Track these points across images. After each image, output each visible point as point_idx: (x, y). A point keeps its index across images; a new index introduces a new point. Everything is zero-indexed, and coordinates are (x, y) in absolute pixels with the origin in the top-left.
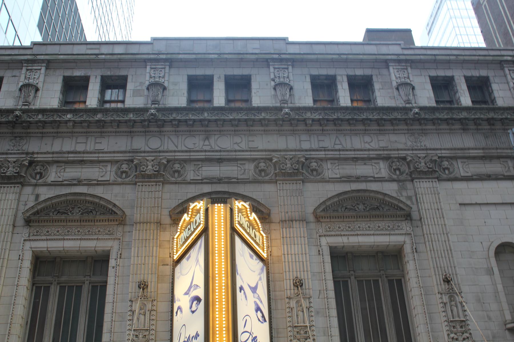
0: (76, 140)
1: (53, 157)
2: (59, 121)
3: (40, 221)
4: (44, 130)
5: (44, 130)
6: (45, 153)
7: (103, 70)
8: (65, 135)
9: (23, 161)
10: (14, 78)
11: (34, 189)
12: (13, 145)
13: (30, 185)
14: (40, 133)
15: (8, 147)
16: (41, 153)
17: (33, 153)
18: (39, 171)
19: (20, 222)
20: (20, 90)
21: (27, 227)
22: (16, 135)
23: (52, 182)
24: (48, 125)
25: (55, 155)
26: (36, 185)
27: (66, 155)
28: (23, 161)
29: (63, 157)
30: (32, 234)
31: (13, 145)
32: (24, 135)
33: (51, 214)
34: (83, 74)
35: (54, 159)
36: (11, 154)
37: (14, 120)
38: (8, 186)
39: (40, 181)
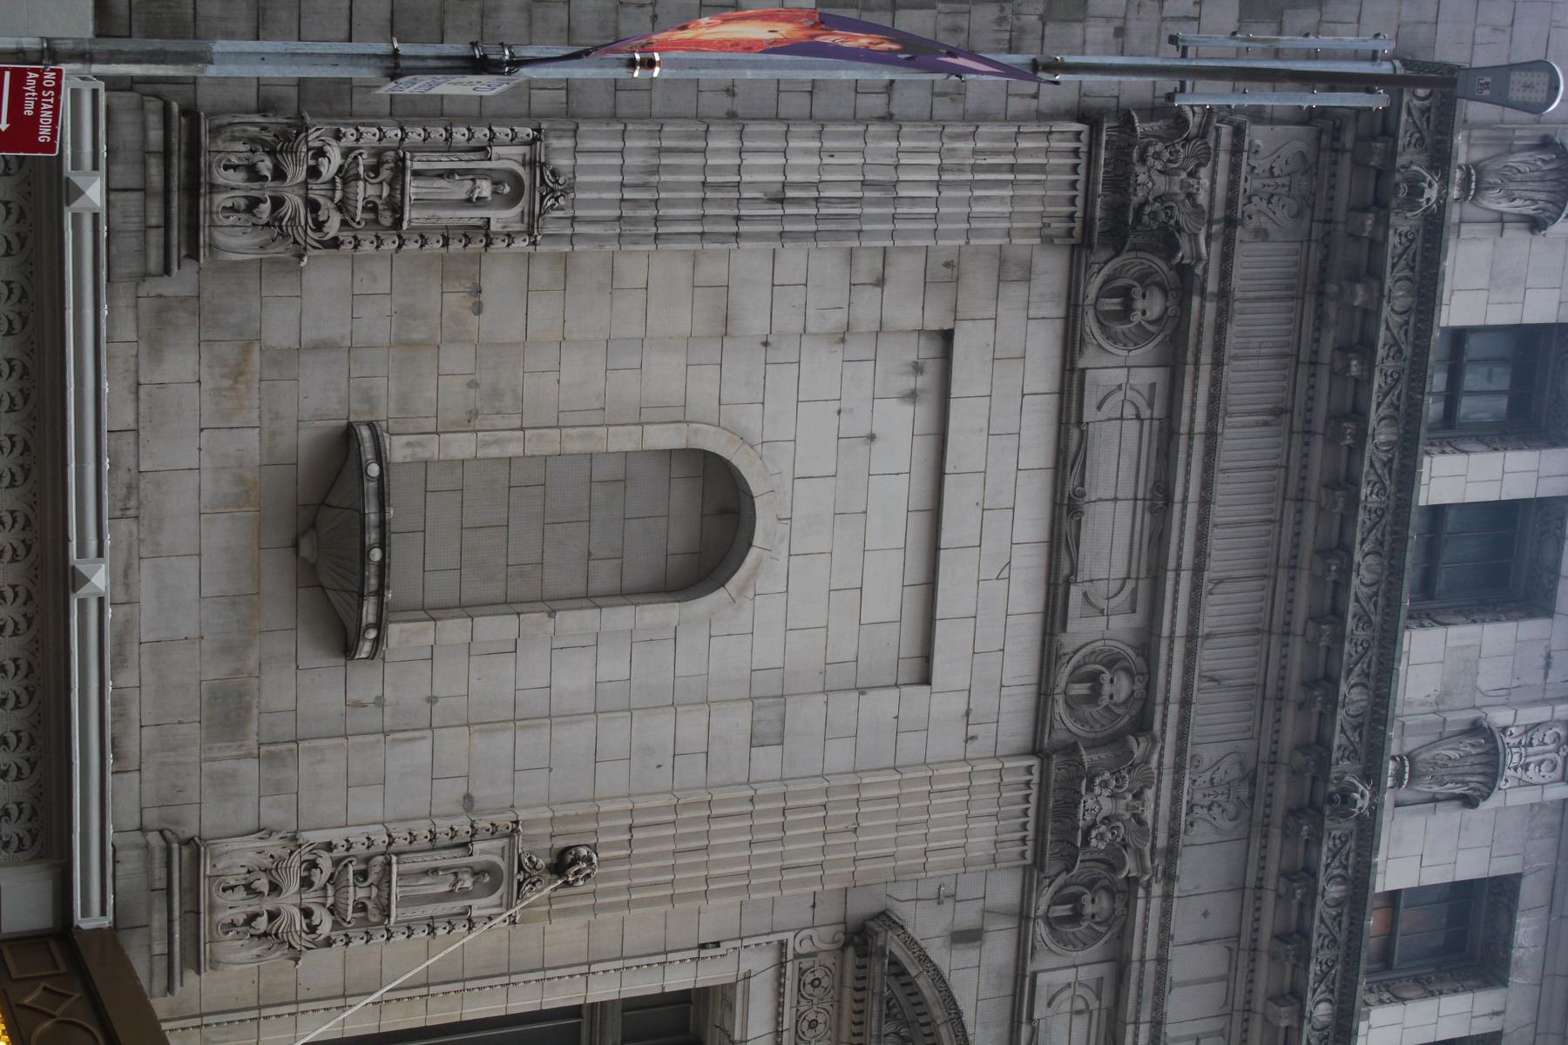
0: (1208, 1035)
1: (1142, 961)
2: (1307, 969)
3: (859, 996)
4: (1269, 898)
5: (1269, 898)
6: (1164, 928)
7: (1531, 1029)
8: (1282, 587)
9: (1139, 854)
10: (1542, 662)
11: (1006, 914)
12: (1217, 777)
13: (1026, 893)
14: (1260, 879)
15: (1208, 754)
16: (1166, 913)
17: (1170, 877)
18: (1089, 909)
19: (861, 906)
20: (1476, 728)
21: (841, 936)
22: (1262, 778)
23: (1034, 975)
24: (1371, 186)
25: (1150, 967)
26: (1023, 916)
27: (1146, 1015)
28: (1139, 854)
29: (1139, 1003)
30: (806, 963)
31: (1217, 777)
32: (1259, 810)
33: (889, 1028)
34: (1516, 954)
35: (1135, 966)
36: (1177, 785)
37: (1332, 788)
38: (1032, 813)
39: (1042, 929)
